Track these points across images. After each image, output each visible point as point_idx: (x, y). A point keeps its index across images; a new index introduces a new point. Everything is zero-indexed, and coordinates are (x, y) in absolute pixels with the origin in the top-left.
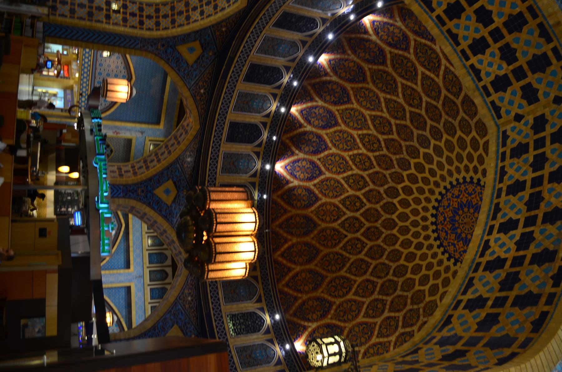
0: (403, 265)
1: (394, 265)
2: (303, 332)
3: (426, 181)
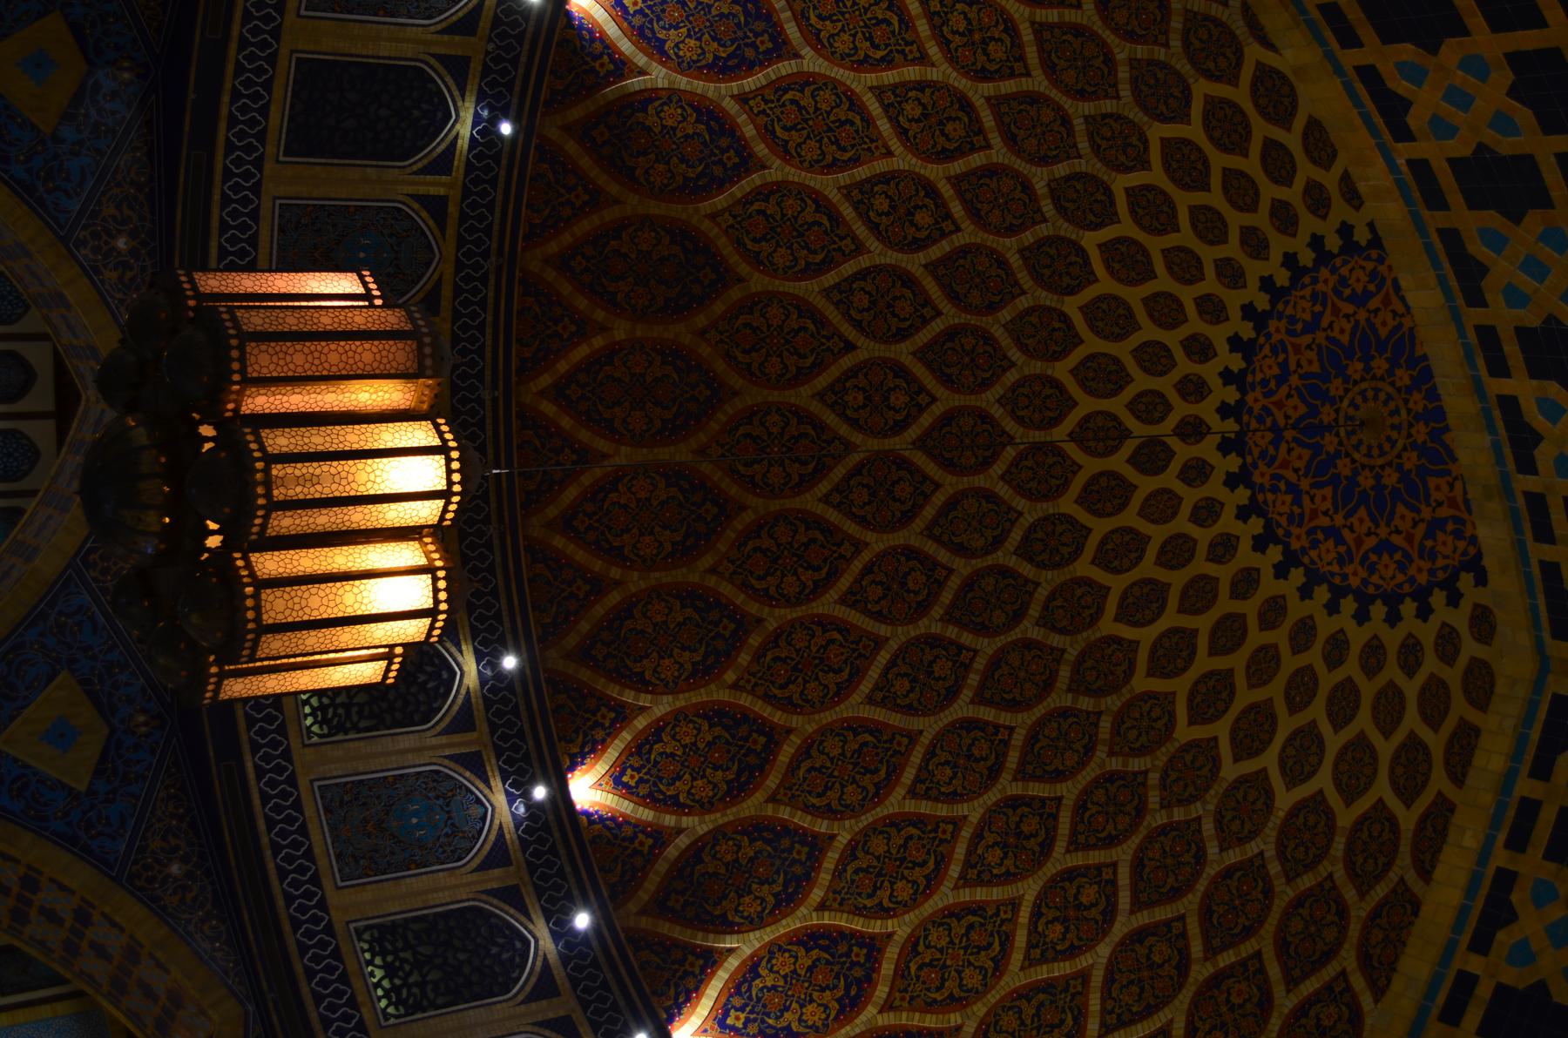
0: (1069, 520)
1: (1030, 512)
2: (612, 733)
3: (1241, 191)
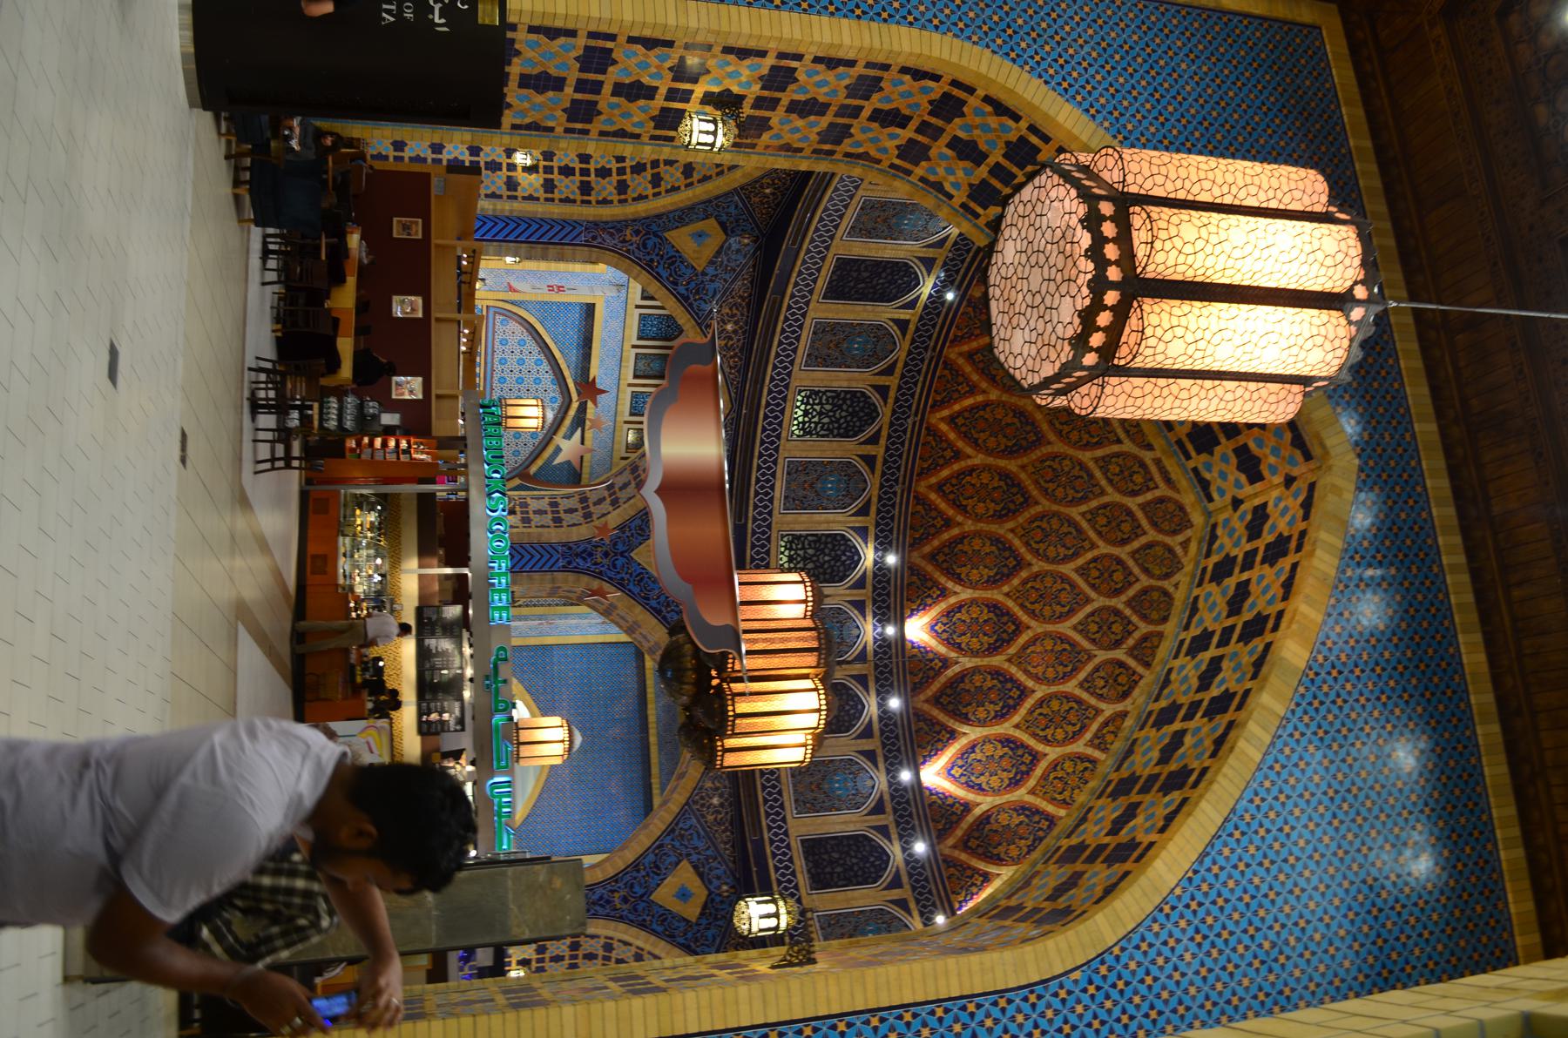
2: (936, 602)
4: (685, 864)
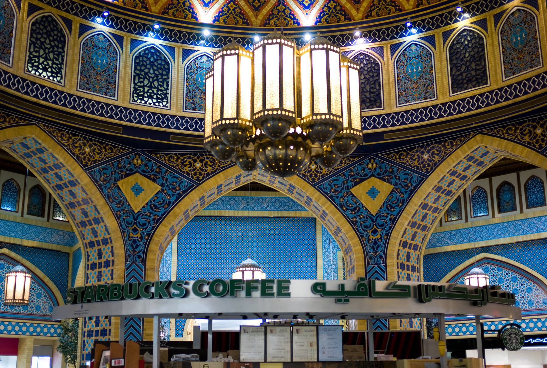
4: (353, 191)
